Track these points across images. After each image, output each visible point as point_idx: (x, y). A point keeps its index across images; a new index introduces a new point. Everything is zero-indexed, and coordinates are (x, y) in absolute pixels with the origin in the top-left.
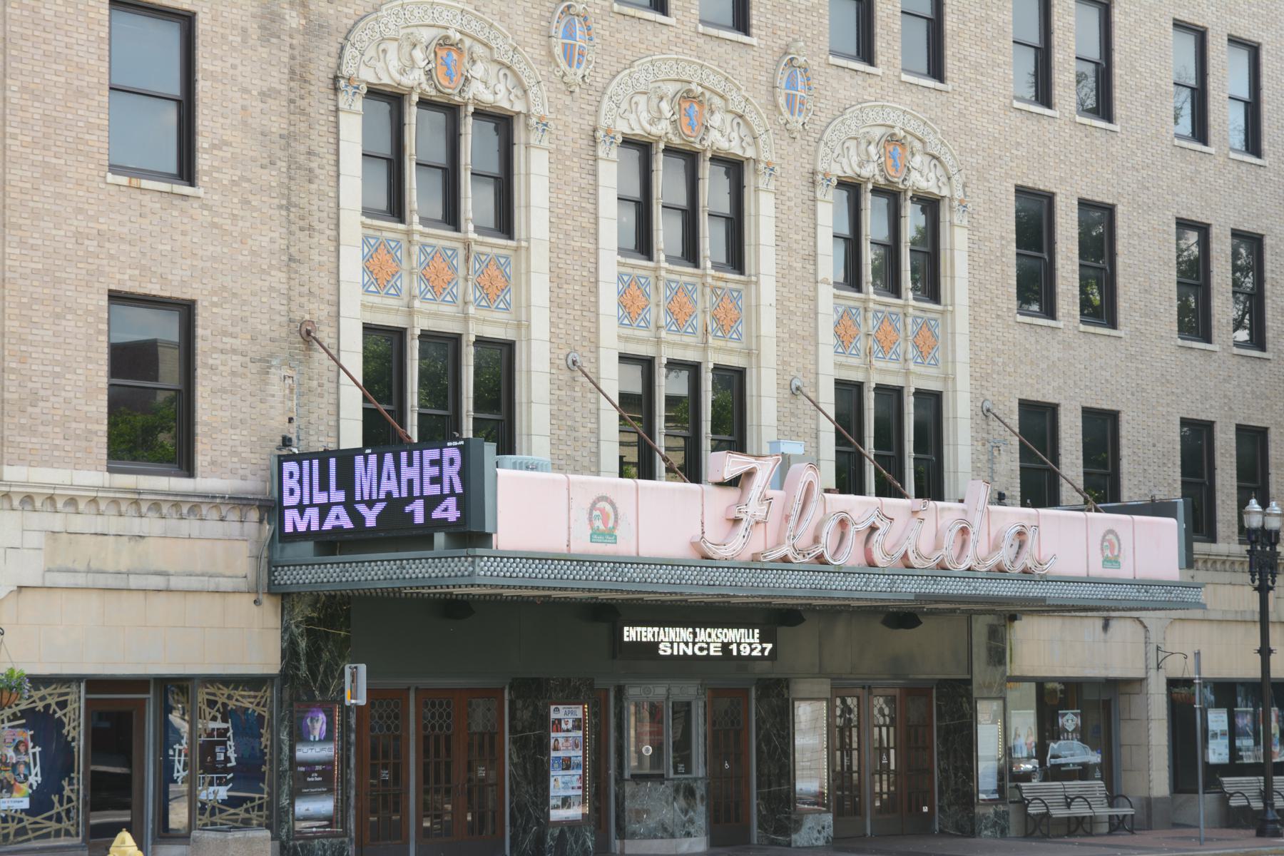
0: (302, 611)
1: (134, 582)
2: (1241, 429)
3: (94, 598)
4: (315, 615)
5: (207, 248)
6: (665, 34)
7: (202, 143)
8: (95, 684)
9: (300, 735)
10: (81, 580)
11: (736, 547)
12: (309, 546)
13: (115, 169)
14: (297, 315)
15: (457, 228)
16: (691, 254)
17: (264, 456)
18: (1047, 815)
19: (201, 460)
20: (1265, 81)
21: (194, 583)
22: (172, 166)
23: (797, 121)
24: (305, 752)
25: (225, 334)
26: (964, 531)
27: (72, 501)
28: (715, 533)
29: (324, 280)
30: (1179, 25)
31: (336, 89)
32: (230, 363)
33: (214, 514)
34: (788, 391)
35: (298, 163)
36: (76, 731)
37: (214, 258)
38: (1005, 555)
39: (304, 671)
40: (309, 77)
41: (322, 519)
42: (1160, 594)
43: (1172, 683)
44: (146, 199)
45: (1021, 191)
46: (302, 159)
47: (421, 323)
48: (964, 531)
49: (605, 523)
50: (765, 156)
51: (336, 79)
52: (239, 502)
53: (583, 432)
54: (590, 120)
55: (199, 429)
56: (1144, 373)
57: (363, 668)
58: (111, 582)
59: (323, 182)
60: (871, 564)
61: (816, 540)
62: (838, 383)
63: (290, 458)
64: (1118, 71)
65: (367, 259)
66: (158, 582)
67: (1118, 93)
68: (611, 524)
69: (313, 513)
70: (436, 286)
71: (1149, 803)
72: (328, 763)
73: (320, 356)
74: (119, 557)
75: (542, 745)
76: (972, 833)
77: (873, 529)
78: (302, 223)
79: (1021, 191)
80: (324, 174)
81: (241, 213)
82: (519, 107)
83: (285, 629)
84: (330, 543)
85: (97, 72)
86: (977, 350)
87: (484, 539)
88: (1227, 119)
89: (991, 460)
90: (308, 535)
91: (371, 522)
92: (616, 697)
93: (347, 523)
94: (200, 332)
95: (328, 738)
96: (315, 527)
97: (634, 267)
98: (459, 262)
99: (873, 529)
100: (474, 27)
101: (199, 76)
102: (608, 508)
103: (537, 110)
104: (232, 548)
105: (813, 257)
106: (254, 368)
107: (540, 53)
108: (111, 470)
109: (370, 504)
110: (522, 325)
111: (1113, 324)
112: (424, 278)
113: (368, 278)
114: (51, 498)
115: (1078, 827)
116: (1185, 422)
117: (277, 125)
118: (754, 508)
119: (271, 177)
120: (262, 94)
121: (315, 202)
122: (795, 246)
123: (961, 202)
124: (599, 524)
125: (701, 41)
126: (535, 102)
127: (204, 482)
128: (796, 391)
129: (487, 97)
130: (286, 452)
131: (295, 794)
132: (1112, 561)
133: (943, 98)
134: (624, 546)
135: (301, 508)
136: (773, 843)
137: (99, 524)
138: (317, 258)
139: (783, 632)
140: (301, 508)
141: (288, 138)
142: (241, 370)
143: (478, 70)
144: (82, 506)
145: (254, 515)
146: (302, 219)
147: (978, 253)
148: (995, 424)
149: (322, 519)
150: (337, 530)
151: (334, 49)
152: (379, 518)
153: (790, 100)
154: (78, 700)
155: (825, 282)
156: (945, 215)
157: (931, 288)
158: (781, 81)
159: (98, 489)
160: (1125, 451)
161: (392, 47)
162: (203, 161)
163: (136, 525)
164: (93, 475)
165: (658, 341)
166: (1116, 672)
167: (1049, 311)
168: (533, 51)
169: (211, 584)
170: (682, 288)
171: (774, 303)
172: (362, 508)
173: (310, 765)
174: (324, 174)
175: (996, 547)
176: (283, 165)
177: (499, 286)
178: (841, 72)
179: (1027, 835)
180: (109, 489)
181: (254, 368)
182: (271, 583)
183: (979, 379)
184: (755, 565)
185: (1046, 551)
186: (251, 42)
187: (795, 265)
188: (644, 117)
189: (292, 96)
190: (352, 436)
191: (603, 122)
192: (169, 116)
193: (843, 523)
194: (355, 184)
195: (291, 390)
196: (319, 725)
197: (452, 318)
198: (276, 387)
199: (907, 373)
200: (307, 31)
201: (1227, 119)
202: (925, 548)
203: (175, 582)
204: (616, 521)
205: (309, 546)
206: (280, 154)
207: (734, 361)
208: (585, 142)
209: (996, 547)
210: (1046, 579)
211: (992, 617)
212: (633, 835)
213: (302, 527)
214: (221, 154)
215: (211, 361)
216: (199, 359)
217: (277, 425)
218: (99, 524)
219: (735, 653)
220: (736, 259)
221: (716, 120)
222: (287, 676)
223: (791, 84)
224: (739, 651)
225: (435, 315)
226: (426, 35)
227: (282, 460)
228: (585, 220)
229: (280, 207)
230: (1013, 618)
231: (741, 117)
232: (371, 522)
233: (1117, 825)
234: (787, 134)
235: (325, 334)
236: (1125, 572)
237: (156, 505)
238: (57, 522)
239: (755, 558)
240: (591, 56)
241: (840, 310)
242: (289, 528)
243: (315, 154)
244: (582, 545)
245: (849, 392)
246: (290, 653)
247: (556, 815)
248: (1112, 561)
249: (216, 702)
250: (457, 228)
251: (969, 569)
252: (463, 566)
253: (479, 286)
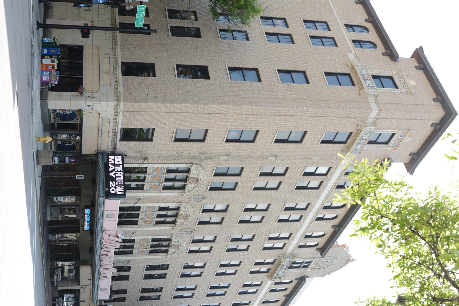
0: (94, 158)
1: (100, 132)
2: (125, 298)
3: (97, 125)
5: (162, 143)
6: (198, 212)
7: (181, 143)
8: (81, 125)
9: (70, 158)
10: (101, 123)
11: (105, 236)
12: (106, 161)
13: (177, 130)
14: (149, 158)
15: (165, 181)
16: (159, 216)
17: (123, 152)
18: (54, 273)
19: (123, 142)
20: (186, 299)
21: (100, 141)
22: (177, 137)
23: (182, 232)
24: (67, 158)
26: (107, 269)
27: (116, 122)
28: (108, 232)
29: (156, 161)
30: (196, 286)
31: (190, 163)
33: (112, 144)
35: (177, 157)
36: (72, 122)
38: (103, 275)
39: (82, 158)
41: (112, 164)
42: (95, 297)
43: (79, 290)
44: (171, 134)
45: (168, 265)
47: (147, 176)
48: (107, 269)
50: (176, 228)
51: (192, 163)
52: (115, 148)
53: (126, 201)
54: (183, 201)
55: (129, 142)
56: (136, 283)
57: (83, 178)
58: (100, 128)
59: (173, 161)
60: (101, 255)
61: (106, 247)
62: (134, 240)
63: (122, 158)
64: (189, 278)
65: (159, 168)
66: (100, 135)
67: (185, 278)
69: (113, 162)
70: (154, 178)
71: (57, 286)
72: (65, 161)
73: (142, 161)
74: (105, 129)
75: (68, 195)
76: (51, 261)
77: (108, 256)
79: (168, 265)
80: (175, 161)
82: (186, 191)
83: (90, 155)
84: (107, 165)
85: (195, 128)
86: (140, 260)
87: (107, 197)
88: (180, 293)
89: (120, 262)
90: (108, 161)
91: (111, 174)
93: (110, 169)
94: (147, 142)
95: (70, 162)
96: (110, 163)
98: (158, 181)
99: (108, 256)
100: (200, 184)
101: (193, 143)
103: (185, 194)
104: (106, 146)
105: (158, 235)
106: (140, 151)
107: (195, 194)
108: (121, 128)
109: (115, 174)
110: (146, 191)
111: (144, 279)
112: (155, 176)
113: (155, 168)
114: (116, 119)
115: (52, 277)
116: (126, 290)
117: (184, 155)
118: (112, 238)
119: (175, 154)
126: (187, 194)
127: (119, 143)
128: (133, 233)
129: (188, 186)
130: (123, 156)
131: (59, 157)
132: (101, 290)
134: (105, 219)
135: (114, 160)
136: (49, 230)
137: (111, 126)
139: (89, 232)
140: (114, 160)
141: (182, 156)
143: (193, 185)
144: (115, 124)
145: (112, 150)
146: (167, 159)
147: (158, 259)
148: (127, 263)
149: (112, 164)
150: (109, 167)
151: (197, 163)
152: (112, 176)
153: (186, 231)
154: (78, 122)
156: (164, 254)
157: (151, 252)
158: (189, 230)
159: (118, 127)
160: (121, 281)
161: (198, 172)
162: (178, 143)
163: (111, 132)
164: (120, 125)
165: (143, 212)
166: (81, 281)
167: (147, 270)
168: (196, 193)
169: (99, 143)
170: (153, 215)
172: (114, 172)
173: (65, 159)
174: (175, 161)
175: (104, 273)
177: (154, 188)
179: (51, 270)
180: (118, 128)
181: (140, 151)
182: (99, 153)
183: (135, 260)
184: (102, 238)
185: (103, 280)
188: (184, 210)
190: (126, 166)
191: (183, 204)
192: (187, 137)
193: (109, 251)
194: (173, 166)
196: (72, 160)
198: (136, 154)
199: (136, 249)
200: (201, 159)
201: (180, 293)
202: (104, 263)
203: (100, 138)
205: (106, 161)
207: (139, 223)
208: (179, 201)
209: (104, 273)
210: (98, 281)
211: (91, 262)
212: (51, 208)
213: (110, 160)
216: (141, 142)
217: (129, 154)
218: (111, 126)
220: (158, 223)
221: (183, 221)
222: (82, 155)
223: (188, 231)
225: (149, 178)
226: (200, 177)
227: (122, 155)
228: (165, 201)
230: (91, 266)
232: (111, 174)
233: (52, 283)
235: (146, 161)
236: (99, 292)
237: (114, 135)
238: (112, 119)
239: (103, 238)
240: (195, 202)
242: (110, 157)
244: (105, 213)
245: (133, 241)
246: (86, 156)
247: (55, 198)
248: (101, 290)
250: (165, 181)
252: (102, 195)
253: (154, 185)
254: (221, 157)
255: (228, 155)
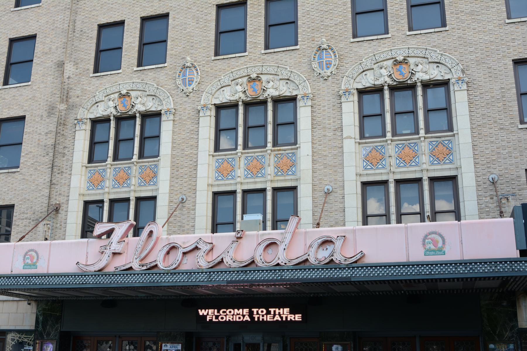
4: (47, 307)
25: (23, 213)
32: (24, 223)
34: (323, 192)
37: (22, 189)
40: (66, 123)
46: (60, 151)
49: (32, 261)
68: (35, 261)
78: (59, 171)
81: (34, 173)
92: (227, 341)
97: (225, 155)
102: (34, 254)
117: (51, 142)
120: (47, 133)
121: (65, 163)
122: (327, 126)
123: (459, 79)
124: (29, 261)
125: (266, 56)
133: (445, 34)
138: (63, 182)
142: (28, 224)
153: (320, 64)
155: (349, 137)
171: (311, 154)
176: (51, 154)
178: (360, 43)
186: (44, 119)
187: (327, 134)
189: (59, 131)
195: (49, 228)
197: (126, 192)
200: (67, 109)
204: (38, 259)
206: (51, 151)
214: (29, 156)
215: (17, 223)
219: (256, 319)
224: (259, 318)
229: (49, 168)
231: (288, 79)
234: (321, 79)
235: (64, 207)
241: (369, 149)
243: (67, 148)
249: (14, 339)
251: (278, 265)
254: (66, 75)
255: (61, 65)
